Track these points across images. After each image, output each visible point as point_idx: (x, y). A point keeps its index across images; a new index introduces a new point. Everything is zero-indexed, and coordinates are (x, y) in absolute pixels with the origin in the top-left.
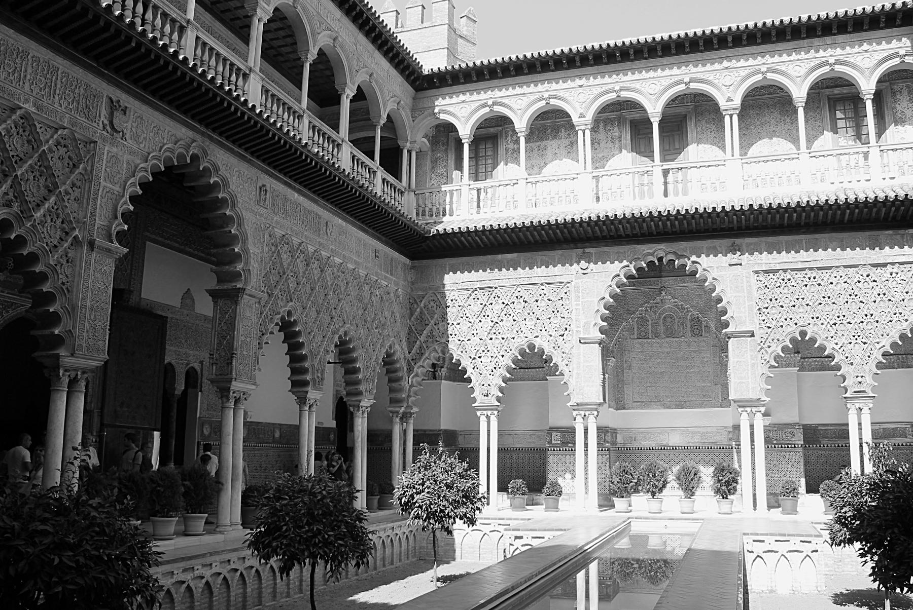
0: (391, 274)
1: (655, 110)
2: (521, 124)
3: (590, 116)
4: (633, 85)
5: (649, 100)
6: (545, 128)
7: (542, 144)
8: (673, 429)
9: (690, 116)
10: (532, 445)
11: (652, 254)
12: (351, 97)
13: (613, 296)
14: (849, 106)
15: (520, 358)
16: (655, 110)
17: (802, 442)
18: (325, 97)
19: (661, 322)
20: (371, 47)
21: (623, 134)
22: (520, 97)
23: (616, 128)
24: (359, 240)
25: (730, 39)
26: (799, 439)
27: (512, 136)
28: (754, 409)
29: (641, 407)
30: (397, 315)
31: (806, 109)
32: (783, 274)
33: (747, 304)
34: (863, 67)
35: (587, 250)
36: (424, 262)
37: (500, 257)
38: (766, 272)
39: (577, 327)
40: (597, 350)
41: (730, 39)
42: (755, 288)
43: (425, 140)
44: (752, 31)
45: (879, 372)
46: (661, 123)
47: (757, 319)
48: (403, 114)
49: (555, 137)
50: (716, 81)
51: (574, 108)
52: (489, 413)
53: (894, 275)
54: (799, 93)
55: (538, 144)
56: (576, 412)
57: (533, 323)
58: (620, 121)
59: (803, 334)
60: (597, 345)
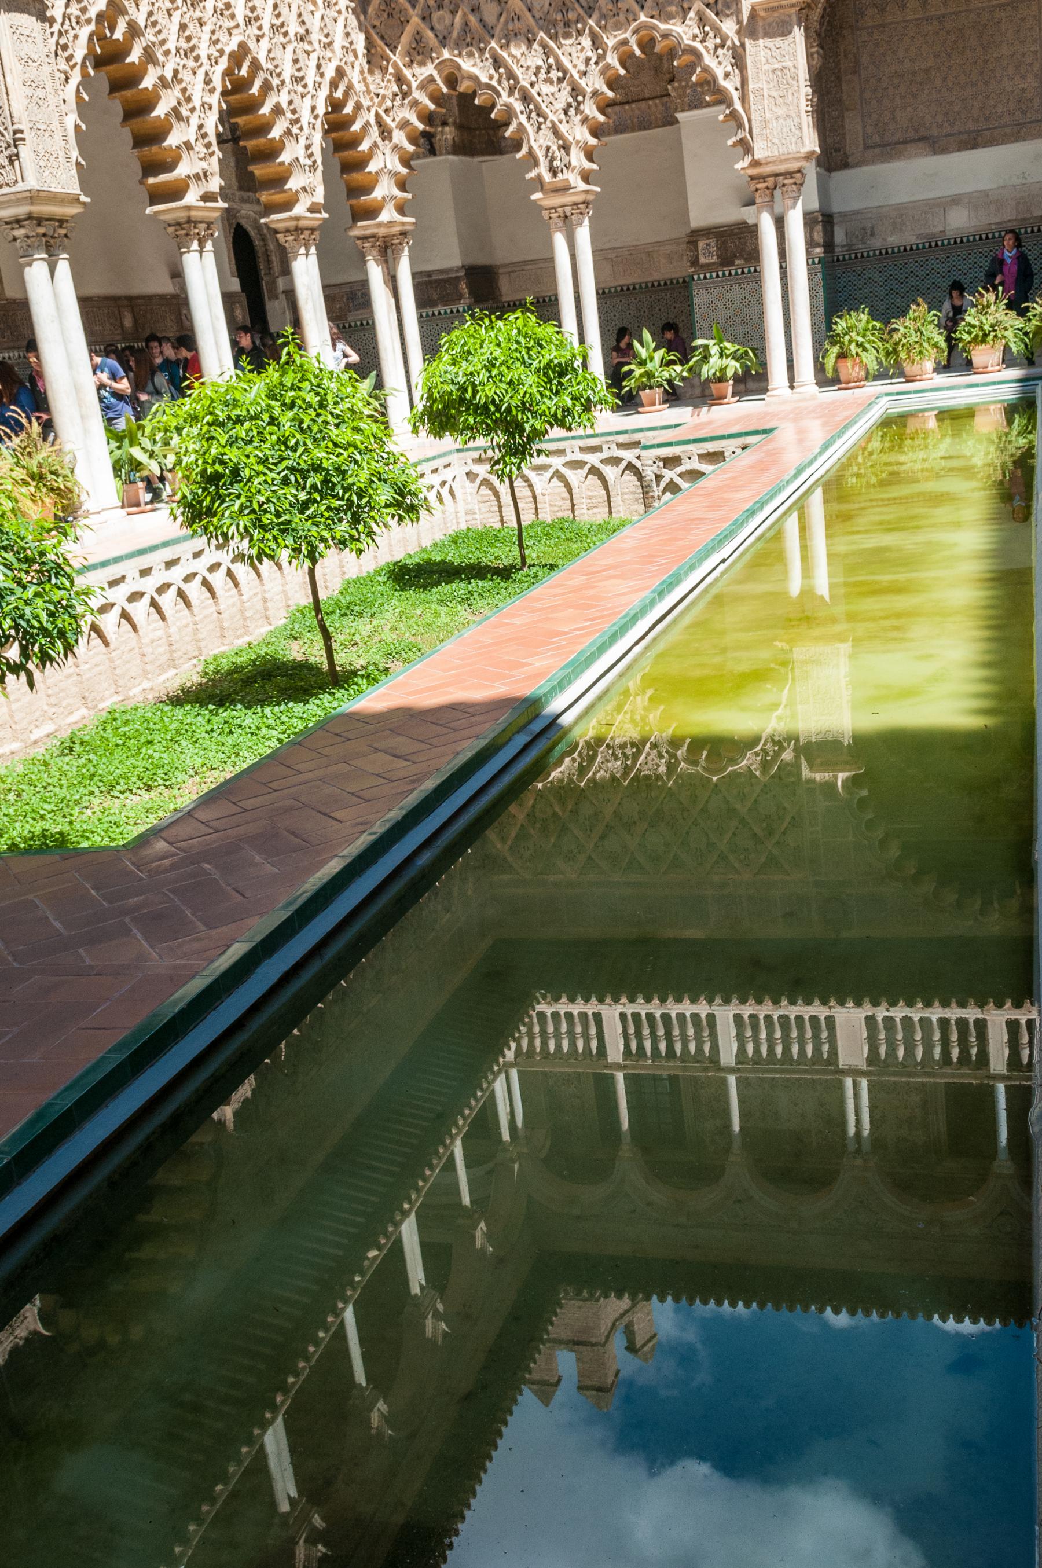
8: (956, 200)
10: (656, 276)
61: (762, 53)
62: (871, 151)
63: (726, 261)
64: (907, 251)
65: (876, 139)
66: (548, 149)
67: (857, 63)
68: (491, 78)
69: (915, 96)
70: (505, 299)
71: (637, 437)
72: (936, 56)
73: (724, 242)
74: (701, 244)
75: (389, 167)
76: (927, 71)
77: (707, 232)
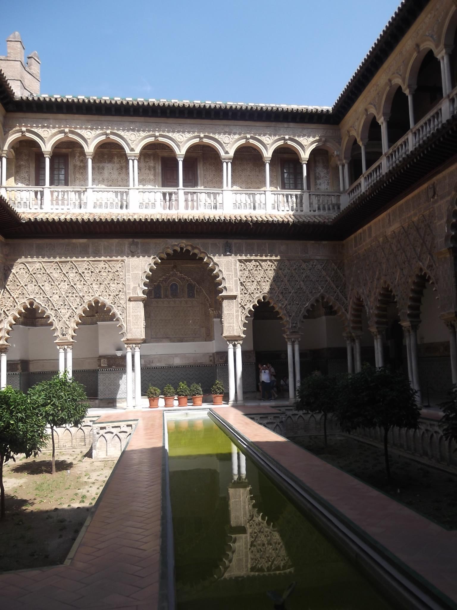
2: (90, 149)
3: (138, 151)
5: (178, 146)
7: (101, 165)
8: (176, 355)
9: (203, 160)
13: (151, 270)
15: (88, 309)
16: (181, 152)
17: (255, 361)
19: (169, 288)
21: (157, 166)
25: (230, 114)
26: (253, 359)
31: (270, 164)
35: (136, 240)
36: (16, 241)
37: (74, 241)
40: (141, 304)
41: (230, 114)
42: (238, 270)
45: (304, 320)
46: (184, 162)
50: (220, 140)
51: (128, 144)
54: (268, 154)
55: (98, 165)
57: (97, 286)
58: (155, 157)
63: (110, 366)
64: (163, 368)
74: (102, 361)
77: (104, 357)
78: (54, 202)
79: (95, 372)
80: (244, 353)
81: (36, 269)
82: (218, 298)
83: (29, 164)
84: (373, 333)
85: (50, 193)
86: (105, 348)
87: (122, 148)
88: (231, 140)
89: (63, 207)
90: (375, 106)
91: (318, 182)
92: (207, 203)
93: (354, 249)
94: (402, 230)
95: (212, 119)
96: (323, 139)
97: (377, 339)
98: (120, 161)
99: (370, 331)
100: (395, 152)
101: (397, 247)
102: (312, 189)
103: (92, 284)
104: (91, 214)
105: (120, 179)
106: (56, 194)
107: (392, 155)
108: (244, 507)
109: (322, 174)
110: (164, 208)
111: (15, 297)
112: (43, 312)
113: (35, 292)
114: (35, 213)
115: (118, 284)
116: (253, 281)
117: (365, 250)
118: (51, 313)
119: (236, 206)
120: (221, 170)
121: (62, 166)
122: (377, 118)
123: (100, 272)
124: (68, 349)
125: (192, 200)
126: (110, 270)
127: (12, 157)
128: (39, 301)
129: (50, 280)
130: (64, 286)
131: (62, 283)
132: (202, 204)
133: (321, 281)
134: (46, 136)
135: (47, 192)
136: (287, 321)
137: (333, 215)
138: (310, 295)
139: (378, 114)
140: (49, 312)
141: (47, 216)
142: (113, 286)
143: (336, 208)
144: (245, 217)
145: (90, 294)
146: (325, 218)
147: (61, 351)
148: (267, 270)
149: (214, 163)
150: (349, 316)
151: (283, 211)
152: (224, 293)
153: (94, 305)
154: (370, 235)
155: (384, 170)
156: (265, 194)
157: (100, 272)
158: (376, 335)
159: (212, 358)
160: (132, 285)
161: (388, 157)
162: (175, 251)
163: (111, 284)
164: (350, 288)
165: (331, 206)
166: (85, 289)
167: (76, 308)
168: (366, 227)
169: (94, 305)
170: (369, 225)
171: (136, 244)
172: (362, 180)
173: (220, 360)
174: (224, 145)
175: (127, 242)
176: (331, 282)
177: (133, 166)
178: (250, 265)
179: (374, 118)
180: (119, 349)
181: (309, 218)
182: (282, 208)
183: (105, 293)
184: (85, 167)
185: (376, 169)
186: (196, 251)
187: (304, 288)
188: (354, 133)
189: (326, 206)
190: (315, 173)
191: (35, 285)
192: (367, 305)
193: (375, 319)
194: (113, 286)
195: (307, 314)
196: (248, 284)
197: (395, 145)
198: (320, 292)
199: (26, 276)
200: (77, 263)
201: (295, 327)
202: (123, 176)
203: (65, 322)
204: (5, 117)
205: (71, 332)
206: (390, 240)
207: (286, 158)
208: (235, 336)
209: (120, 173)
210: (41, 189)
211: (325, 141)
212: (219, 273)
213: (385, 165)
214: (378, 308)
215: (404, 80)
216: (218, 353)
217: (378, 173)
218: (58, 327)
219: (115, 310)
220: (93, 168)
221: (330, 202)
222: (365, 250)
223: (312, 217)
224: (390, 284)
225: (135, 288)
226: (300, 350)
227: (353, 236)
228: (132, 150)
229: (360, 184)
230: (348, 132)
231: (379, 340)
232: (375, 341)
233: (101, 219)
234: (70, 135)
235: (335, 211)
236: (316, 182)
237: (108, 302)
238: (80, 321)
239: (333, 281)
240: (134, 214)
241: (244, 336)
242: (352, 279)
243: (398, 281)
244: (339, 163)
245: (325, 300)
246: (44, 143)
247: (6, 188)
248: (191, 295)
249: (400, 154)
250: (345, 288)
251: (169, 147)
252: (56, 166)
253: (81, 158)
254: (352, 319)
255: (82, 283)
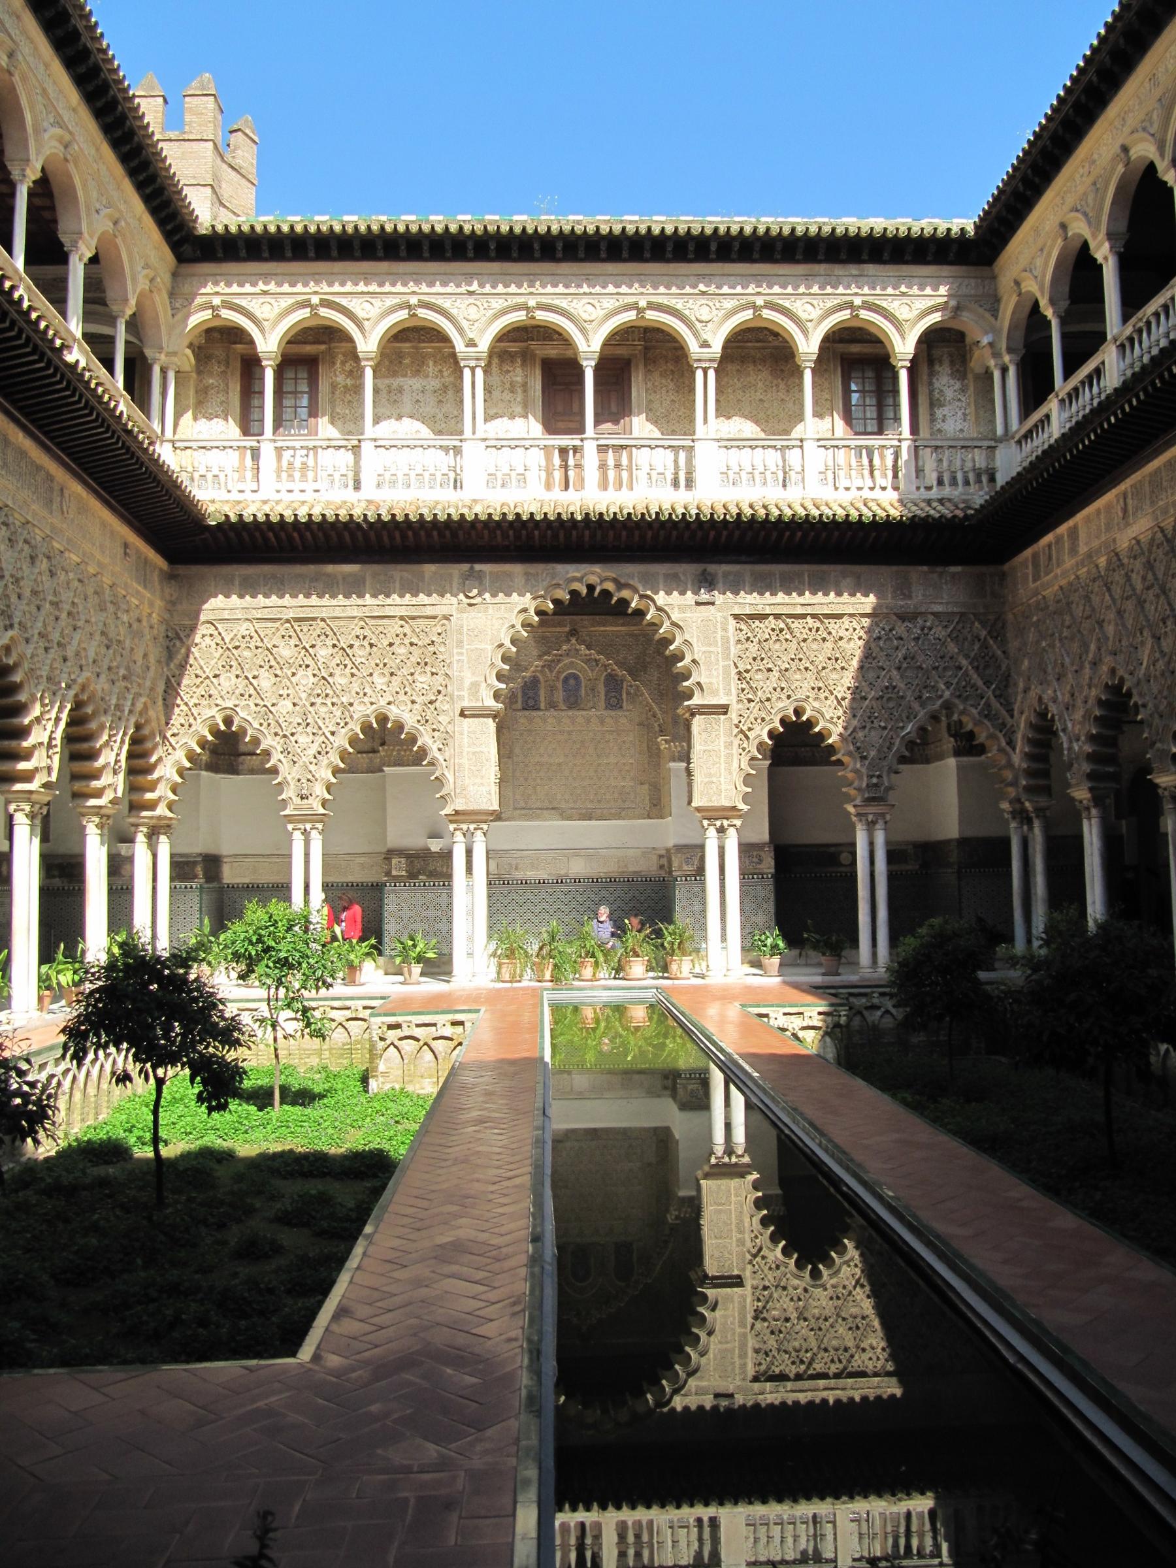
0: (145, 587)
1: (589, 347)
2: (368, 344)
3: (484, 345)
4: (557, 302)
5: (583, 331)
6: (400, 356)
7: (396, 382)
8: (576, 851)
9: (644, 361)
10: (350, 879)
11: (580, 580)
12: (86, 260)
14: (870, 374)
15: (362, 736)
16: (589, 347)
17: (773, 871)
18: (47, 252)
19: (560, 685)
20: (119, 170)
22: (367, 298)
23: (519, 370)
24: (104, 524)
25: (713, 247)
26: (768, 865)
27: (343, 363)
28: (726, 823)
29: (529, 818)
30: (152, 659)
31: (814, 371)
32: (774, 621)
33: (721, 663)
34: (900, 317)
35: (478, 567)
37: (330, 568)
38: (752, 617)
39: (459, 689)
40: (491, 725)
41: (713, 247)
42: (732, 641)
43: (189, 352)
44: (747, 238)
46: (598, 369)
47: (735, 685)
48: (157, 299)
49: (417, 373)
50: (687, 312)
51: (460, 330)
52: (308, 826)
53: (926, 631)
54: (808, 346)
55: (387, 381)
56: (455, 826)
57: (385, 680)
58: (526, 357)
59: (798, 712)
60: (491, 720)
61: (466, 740)
62: (518, 812)
63: (412, 875)
65: (522, 804)
66: (299, 780)
67: (511, 751)
68: (261, 725)
69: (551, 780)
70: (226, 881)
71: (348, 1003)
72: (566, 756)
73: (412, 862)
74: (394, 861)
75: (168, 776)
76: (560, 764)
78: (284, 475)
79: (378, 888)
80: (746, 849)
81: (239, 637)
82: (680, 711)
83: (227, 385)
84: (1081, 802)
85: (273, 453)
86: (404, 832)
87: (445, 339)
88: (715, 312)
89: (303, 486)
90: (1085, 214)
91: (939, 413)
92: (654, 473)
93: (1032, 585)
94: (1159, 535)
95: (668, 261)
96: (953, 303)
97: (1089, 819)
98: (441, 371)
99: (1073, 799)
100: (1140, 331)
101: (1144, 578)
102: (924, 432)
103: (371, 675)
104: (370, 502)
105: (440, 416)
106: (287, 455)
107: (1131, 340)
108: (740, 1222)
109: (949, 394)
110: (548, 486)
111: (191, 704)
112: (256, 741)
113: (237, 692)
114: (239, 502)
115: (433, 674)
116: (770, 670)
117: (1061, 588)
118: (274, 744)
119: (729, 477)
120: (692, 390)
121: (304, 387)
122: (1092, 245)
123: (391, 645)
124: (314, 834)
125: (618, 466)
126: (415, 640)
127: (187, 368)
128: (247, 716)
129: (273, 663)
130: (305, 679)
131: (301, 672)
132: (641, 475)
133: (945, 669)
134: (266, 316)
135: (267, 450)
136: (856, 771)
137: (979, 497)
138: (916, 706)
139: (1094, 236)
140: (267, 742)
141: (266, 509)
142: (423, 680)
143: (984, 479)
144: (751, 506)
145: (366, 700)
146: (957, 508)
147: (297, 835)
148: (805, 640)
149: (673, 372)
150: (1016, 759)
151: (847, 489)
152: (697, 700)
153: (375, 725)
154: (1073, 550)
155: (1112, 380)
156: (801, 447)
157: (391, 645)
158: (1088, 809)
159: (664, 861)
160: (469, 678)
161: (1122, 347)
162: (574, 593)
163: (416, 676)
164: (1021, 685)
165: (971, 476)
166: (356, 687)
167: (333, 733)
168: (1062, 529)
169: (375, 725)
170: (1071, 523)
171: (480, 577)
172: (1052, 405)
173: (686, 868)
174: (698, 325)
175: (457, 570)
176: (971, 672)
177: (474, 383)
178: (762, 629)
179: (1085, 246)
180: (435, 835)
181: (914, 508)
182: (843, 482)
183: (402, 697)
184: (358, 389)
185: (1090, 377)
186: (625, 594)
187: (902, 686)
188: (1031, 286)
189: (959, 476)
190: (931, 392)
191: (237, 676)
192: (1064, 730)
193: (1086, 767)
194: (423, 680)
195: (907, 754)
196: (759, 676)
197: (1140, 314)
198: (941, 696)
199: (217, 655)
200: (336, 623)
201: (876, 785)
202: (449, 407)
203: (306, 766)
204: (175, 275)
205: (320, 790)
206: (1125, 561)
207: (856, 358)
208: (724, 809)
209: (440, 401)
210: (255, 444)
211: (958, 309)
212: (684, 648)
213: (1112, 366)
214: (1092, 738)
215: (1161, 148)
216: (680, 848)
217: (1095, 389)
218: (289, 778)
219: (424, 738)
220: (376, 391)
221: (969, 465)
222: (1061, 588)
223: (923, 505)
224: (1126, 676)
225: (475, 686)
226: (888, 843)
227: (1028, 553)
228: (471, 343)
229: (1048, 417)
230: (1017, 283)
231: (1094, 821)
232: (1085, 823)
233: (393, 515)
234: (324, 312)
235: (981, 489)
236: (932, 415)
237: (410, 720)
238: (342, 766)
239: (977, 669)
240: (475, 501)
241: (746, 808)
242: (1026, 662)
243: (1148, 668)
244: (992, 363)
245: (955, 717)
246: (262, 331)
247: (173, 442)
248: (614, 703)
249: (1153, 338)
250: (1006, 686)
251: (560, 334)
252: (288, 386)
253: (348, 367)
254: (1025, 765)
255: (348, 671)
